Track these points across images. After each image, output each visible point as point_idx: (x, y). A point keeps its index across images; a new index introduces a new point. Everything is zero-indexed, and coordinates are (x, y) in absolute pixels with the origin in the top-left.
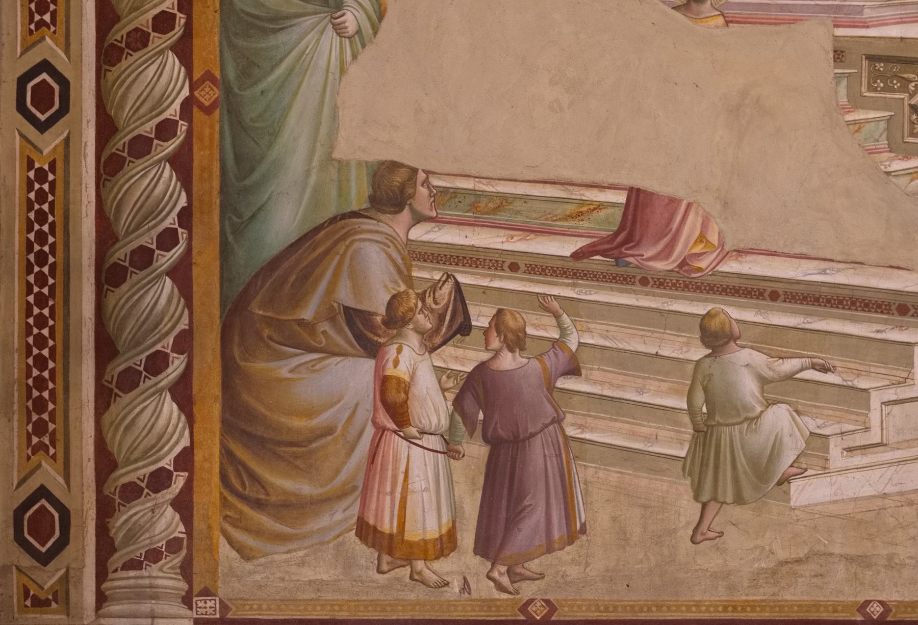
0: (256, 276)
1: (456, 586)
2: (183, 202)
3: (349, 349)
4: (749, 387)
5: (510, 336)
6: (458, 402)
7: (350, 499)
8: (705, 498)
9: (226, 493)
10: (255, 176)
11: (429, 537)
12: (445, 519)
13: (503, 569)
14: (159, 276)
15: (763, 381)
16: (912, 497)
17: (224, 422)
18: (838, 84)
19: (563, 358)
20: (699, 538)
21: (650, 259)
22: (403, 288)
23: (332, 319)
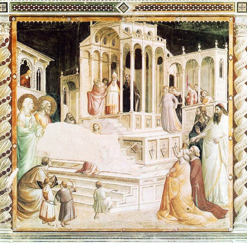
0: (23, 176)
1: (55, 226)
2: (11, 164)
3: (38, 187)
4: (104, 194)
5: (65, 186)
6: (56, 196)
7: (37, 212)
8: (96, 211)
9: (18, 211)
10: (22, 160)
11: (51, 218)
12: (54, 215)
13: (63, 223)
14: (7, 176)
15: (106, 193)
16: (131, 212)
17: (18, 199)
18: (119, 144)
19: (73, 189)
20: (95, 218)
21: (87, 173)
22: (47, 178)
23: (35, 183)
